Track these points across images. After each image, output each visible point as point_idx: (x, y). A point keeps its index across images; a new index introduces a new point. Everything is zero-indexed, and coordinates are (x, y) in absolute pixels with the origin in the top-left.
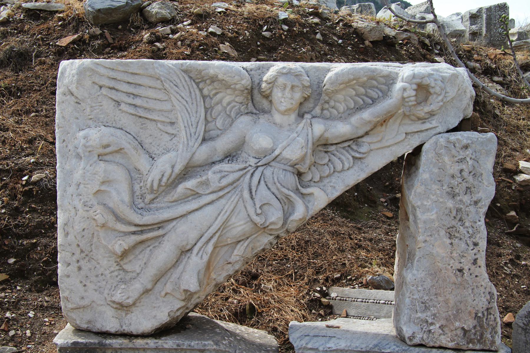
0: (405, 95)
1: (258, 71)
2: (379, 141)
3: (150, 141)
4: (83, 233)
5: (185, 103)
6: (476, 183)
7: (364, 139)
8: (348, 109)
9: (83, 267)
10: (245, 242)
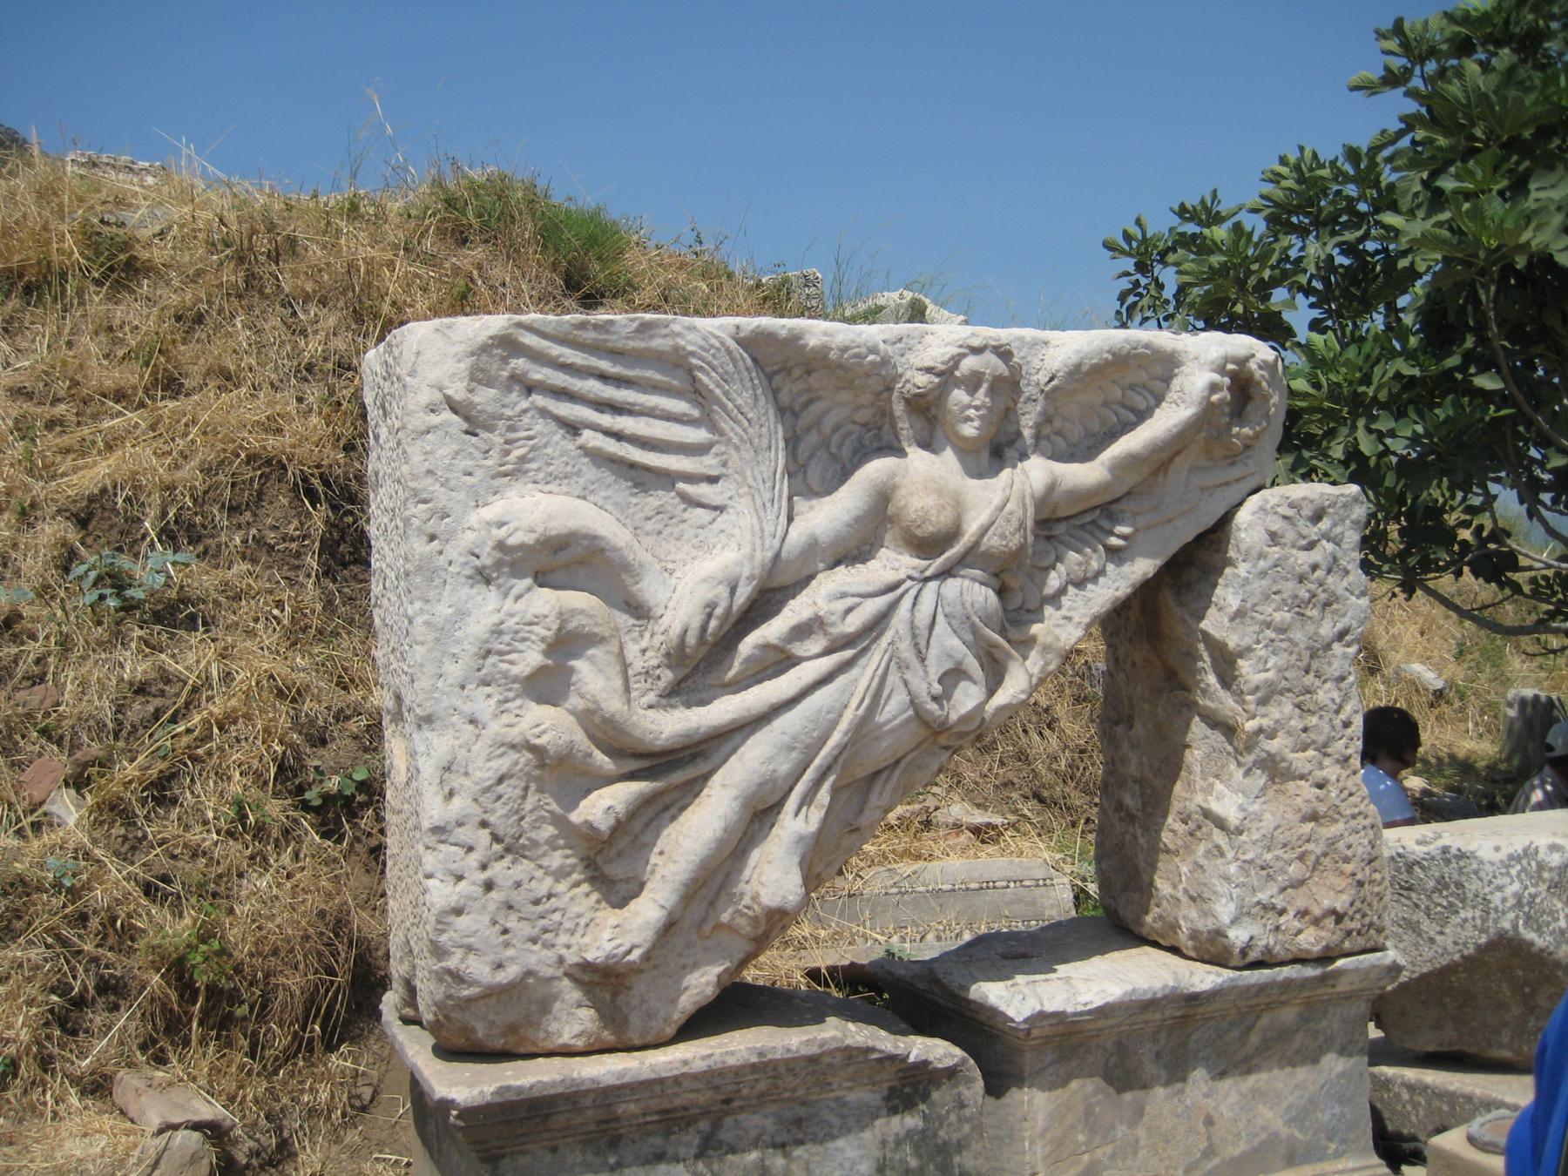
0: (1215, 398)
1: (898, 345)
2: (1154, 509)
3: (659, 526)
4: (501, 789)
5: (746, 424)
6: (1340, 592)
7: (1123, 505)
8: (1090, 435)
9: (499, 881)
10: (892, 773)
